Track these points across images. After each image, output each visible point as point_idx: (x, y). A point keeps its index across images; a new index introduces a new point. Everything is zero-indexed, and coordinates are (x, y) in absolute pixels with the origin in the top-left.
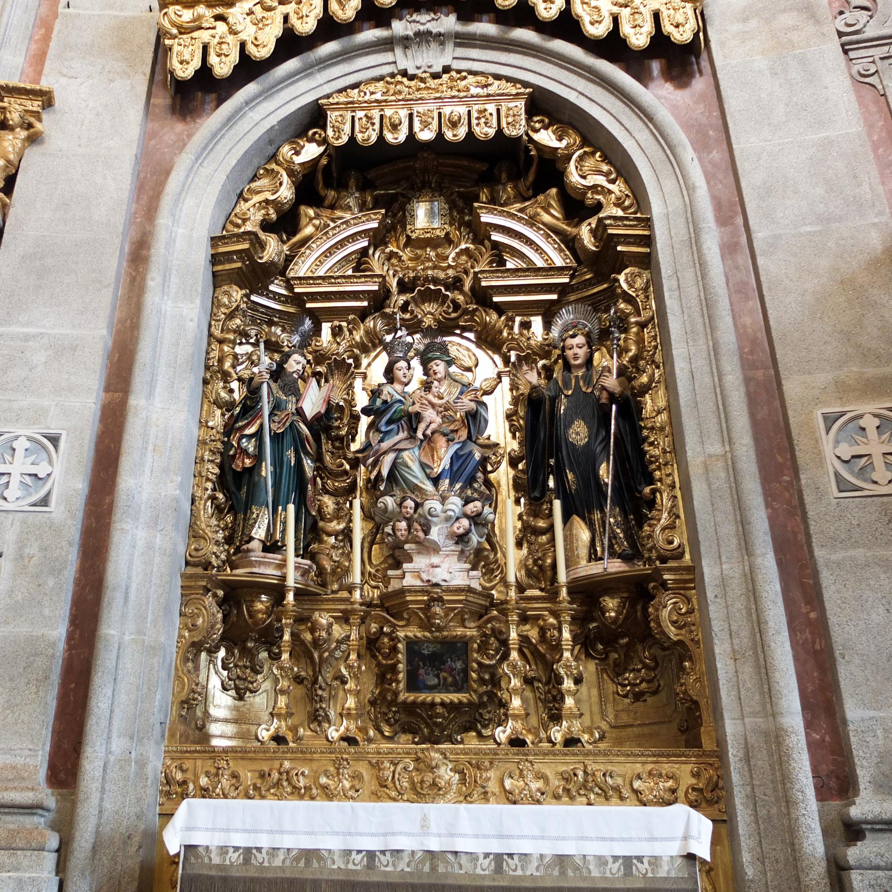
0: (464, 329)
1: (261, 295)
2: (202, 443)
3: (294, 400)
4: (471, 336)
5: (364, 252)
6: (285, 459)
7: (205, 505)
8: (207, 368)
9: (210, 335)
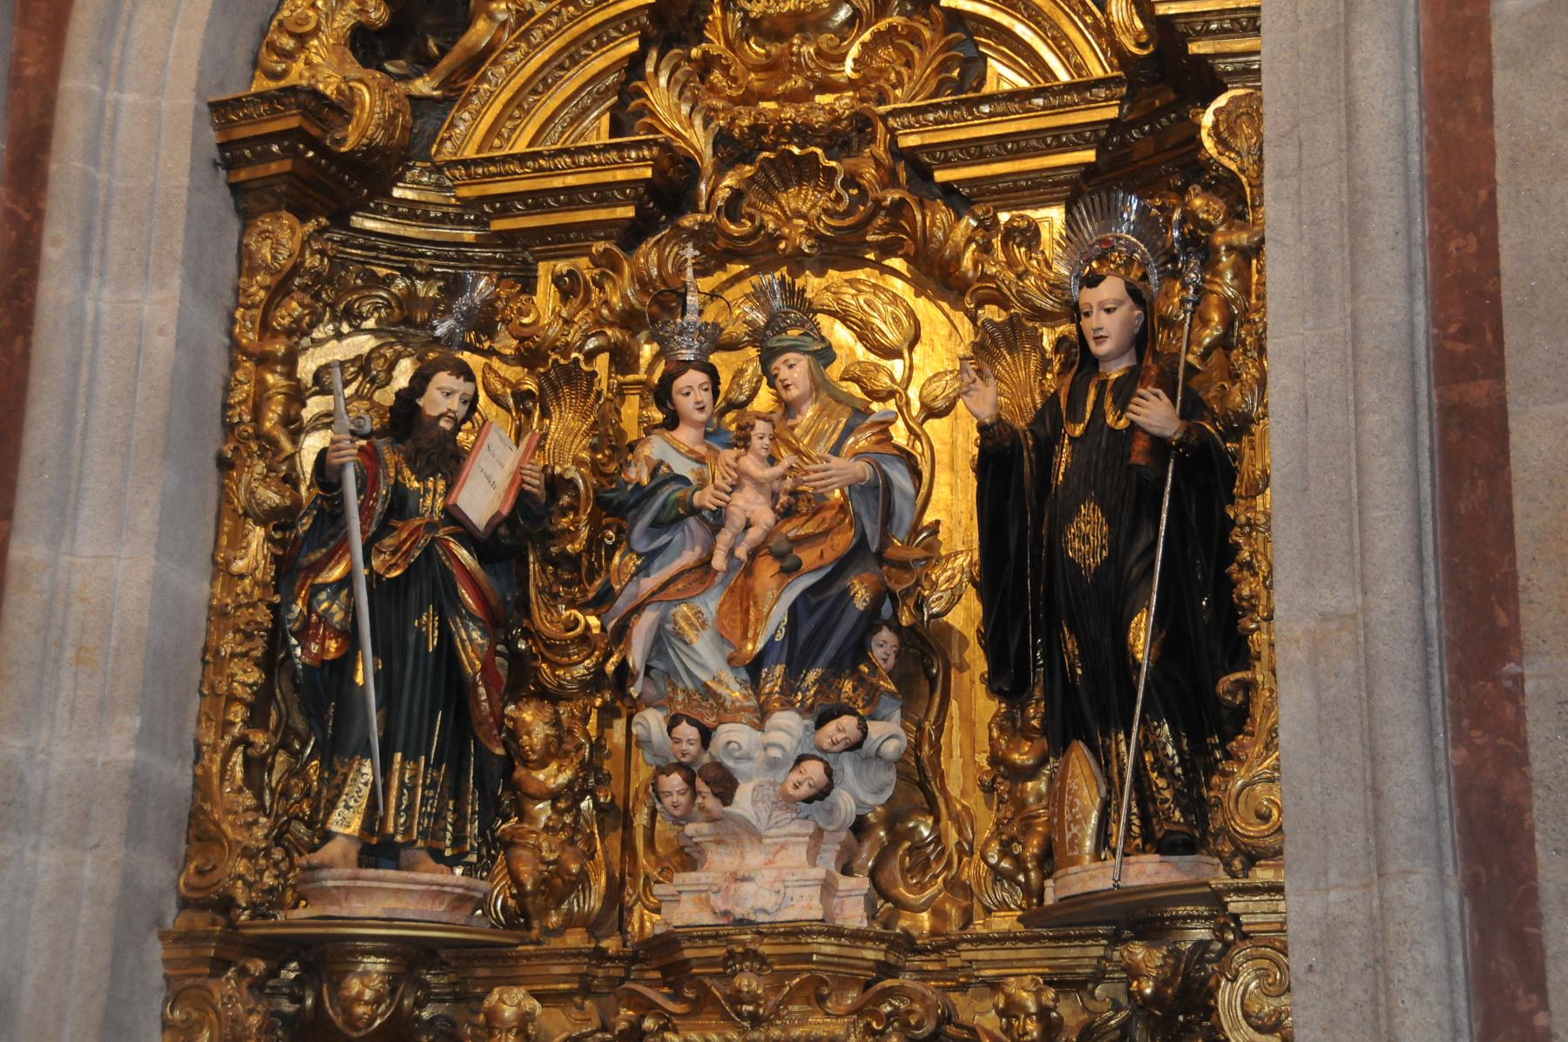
0: (886, 250)
1: (376, 212)
2: (218, 614)
3: (441, 486)
4: (897, 263)
5: (634, 64)
6: (411, 639)
7: (226, 761)
8: (229, 428)
9: (235, 344)
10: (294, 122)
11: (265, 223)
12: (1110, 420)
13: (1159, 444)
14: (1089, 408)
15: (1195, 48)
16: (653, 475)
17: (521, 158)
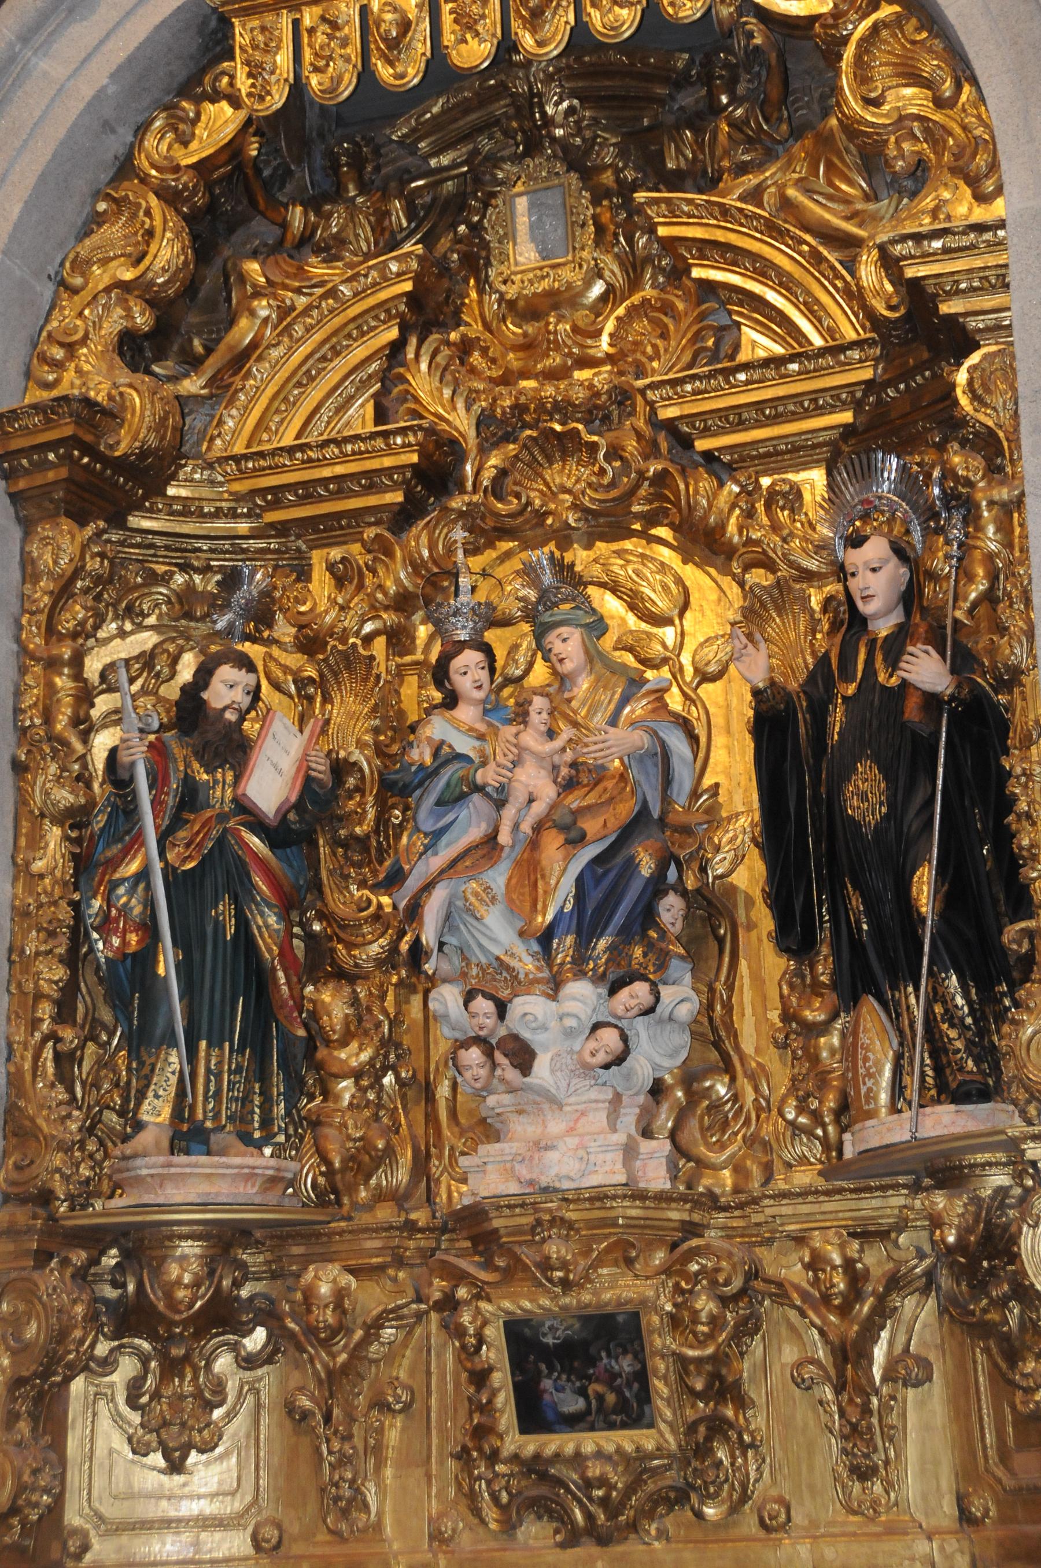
0: (651, 519)
1: (152, 512)
2: (21, 914)
3: (230, 777)
4: (663, 532)
5: (396, 348)
6: (210, 929)
7: (37, 1057)
9: (23, 650)
10: (68, 431)
11: (45, 530)
12: (882, 677)
13: (932, 701)
14: (860, 667)
15: (945, 309)
16: (436, 755)
17: (291, 450)
